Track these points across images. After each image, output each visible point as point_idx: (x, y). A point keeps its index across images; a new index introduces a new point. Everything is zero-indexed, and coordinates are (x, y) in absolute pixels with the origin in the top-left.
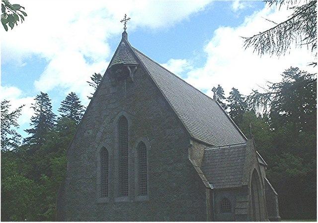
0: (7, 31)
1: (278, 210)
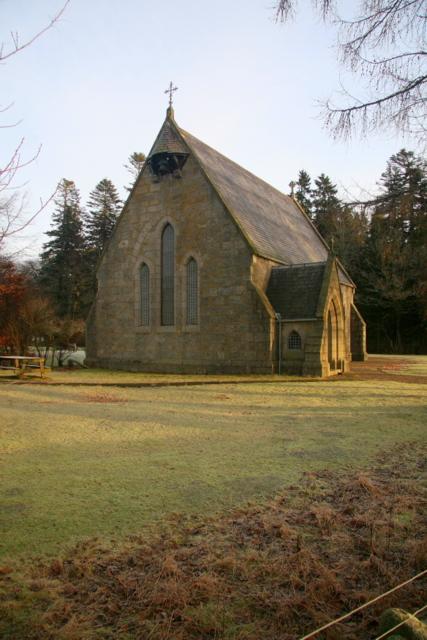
0: (47, 233)
1: (364, 333)
